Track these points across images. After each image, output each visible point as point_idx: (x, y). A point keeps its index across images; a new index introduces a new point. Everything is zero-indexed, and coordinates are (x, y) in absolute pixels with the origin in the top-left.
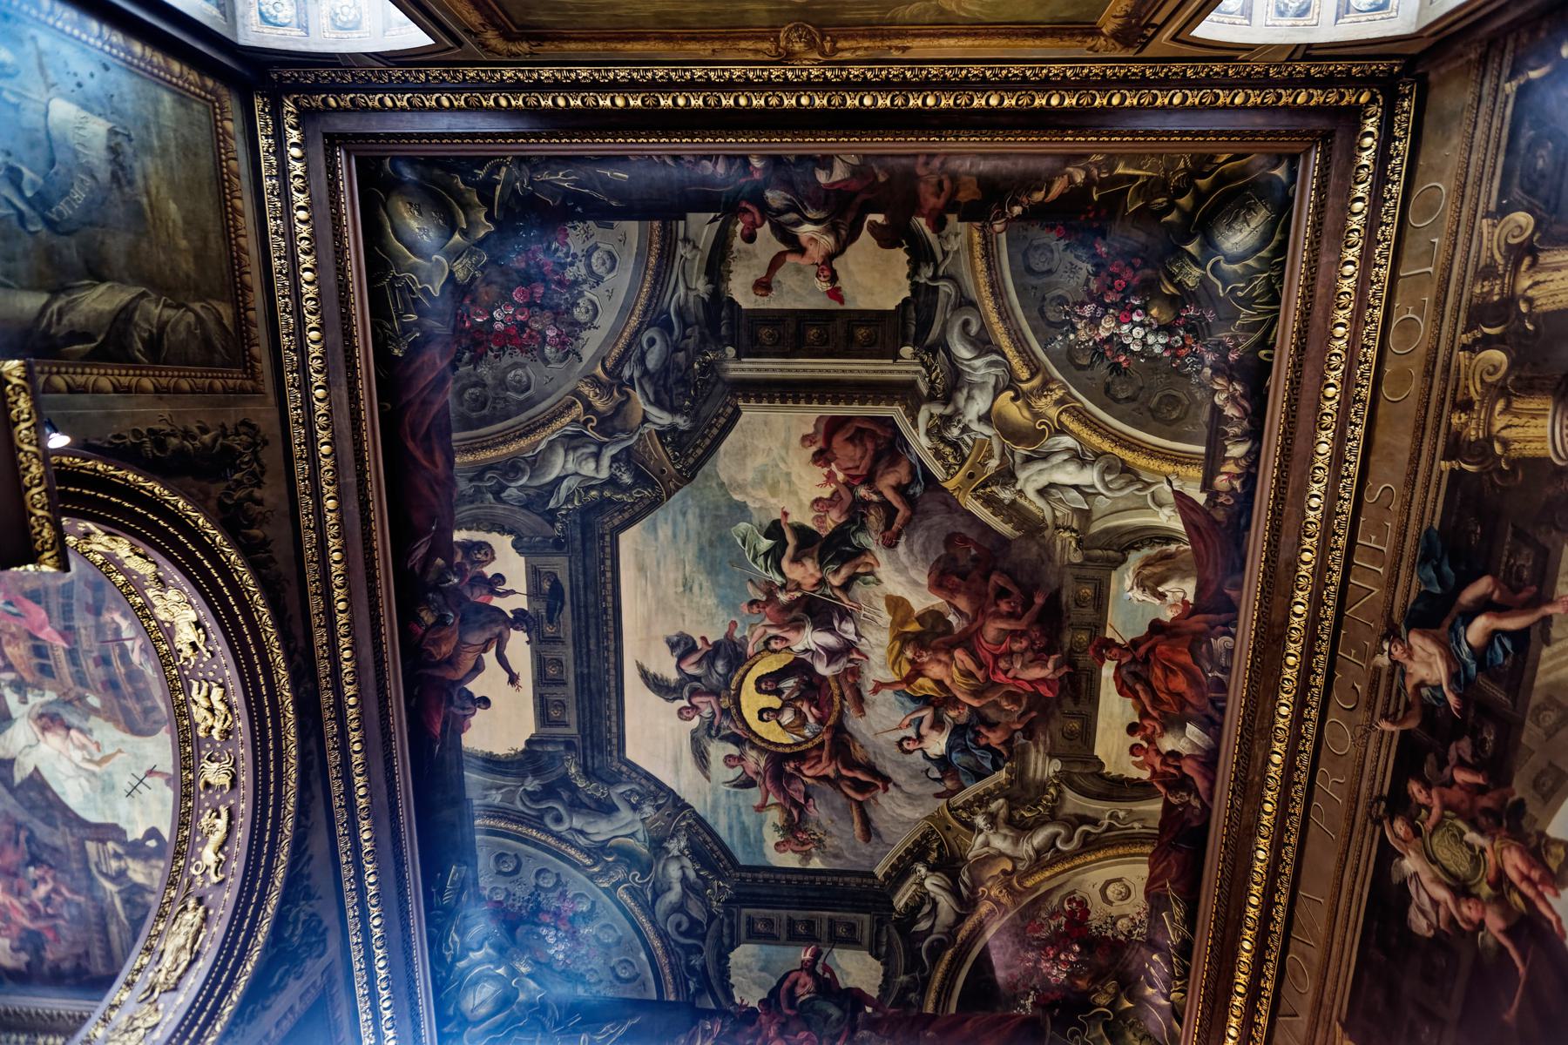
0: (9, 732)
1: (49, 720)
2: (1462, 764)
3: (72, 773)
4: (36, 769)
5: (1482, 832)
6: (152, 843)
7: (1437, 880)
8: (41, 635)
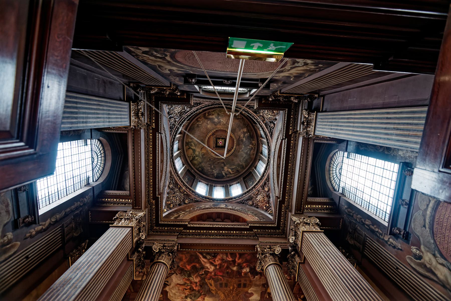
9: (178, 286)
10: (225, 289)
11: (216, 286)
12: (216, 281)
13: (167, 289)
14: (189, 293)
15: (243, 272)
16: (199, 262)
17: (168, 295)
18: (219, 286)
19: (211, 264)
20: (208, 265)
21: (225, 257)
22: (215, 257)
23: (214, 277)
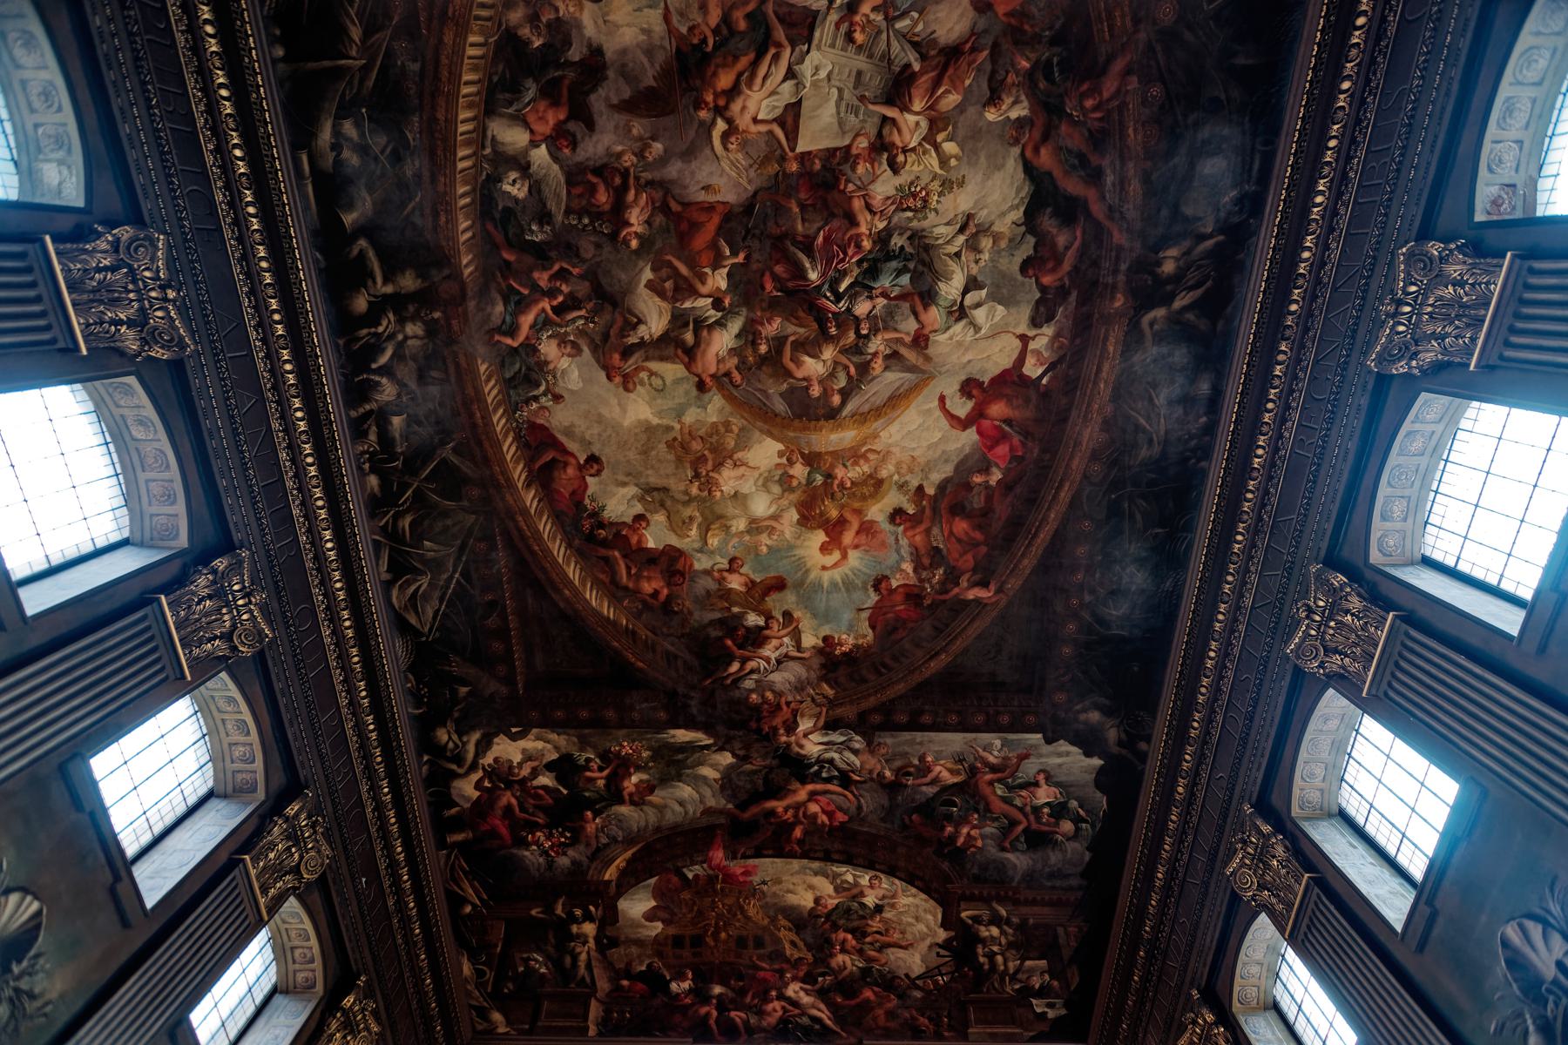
9: (904, 944)
10: (745, 933)
11: (778, 941)
12: (778, 955)
13: (942, 935)
14: (870, 922)
15: (689, 982)
16: (831, 1005)
17: (940, 916)
18: (767, 938)
19: (795, 1003)
20: (806, 999)
21: (753, 1020)
22: (784, 1021)
23: (785, 966)
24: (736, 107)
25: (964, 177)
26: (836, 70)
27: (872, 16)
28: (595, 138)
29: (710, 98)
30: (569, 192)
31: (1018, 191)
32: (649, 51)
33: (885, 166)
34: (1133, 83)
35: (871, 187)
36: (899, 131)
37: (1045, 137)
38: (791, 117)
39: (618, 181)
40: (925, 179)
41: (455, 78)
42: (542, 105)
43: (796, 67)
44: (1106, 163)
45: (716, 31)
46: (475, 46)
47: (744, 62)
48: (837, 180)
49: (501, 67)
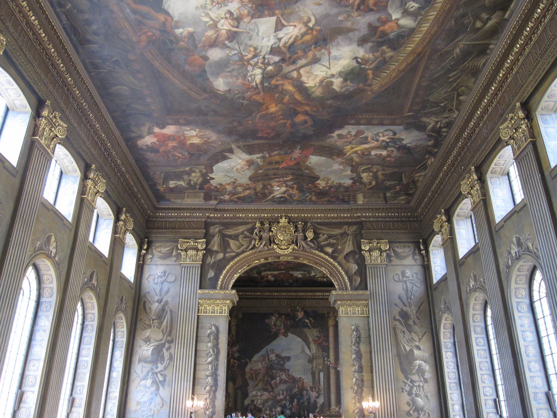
0: (244, 154)
1: (250, 163)
2: (290, 322)
3: (231, 165)
4: (231, 158)
5: (284, 326)
6: (208, 178)
7: (274, 322)
8: (283, 163)
24: (304, 30)
25: (197, 10)
26: (260, 41)
27: (247, 54)
28: (369, 21)
29: (315, 33)
30: (387, 3)
31: (169, 6)
32: (338, 44)
33: (234, 13)
34: (135, 39)
35: (240, 6)
36: (230, 24)
37: (164, 24)
38: (279, 27)
39: (362, 7)
40: (215, 9)
41: (423, 39)
42: (389, 31)
43: (277, 41)
44: (133, 16)
45: (310, 50)
46: (410, 47)
47: (299, 42)
48: (256, 8)
49: (403, 41)
